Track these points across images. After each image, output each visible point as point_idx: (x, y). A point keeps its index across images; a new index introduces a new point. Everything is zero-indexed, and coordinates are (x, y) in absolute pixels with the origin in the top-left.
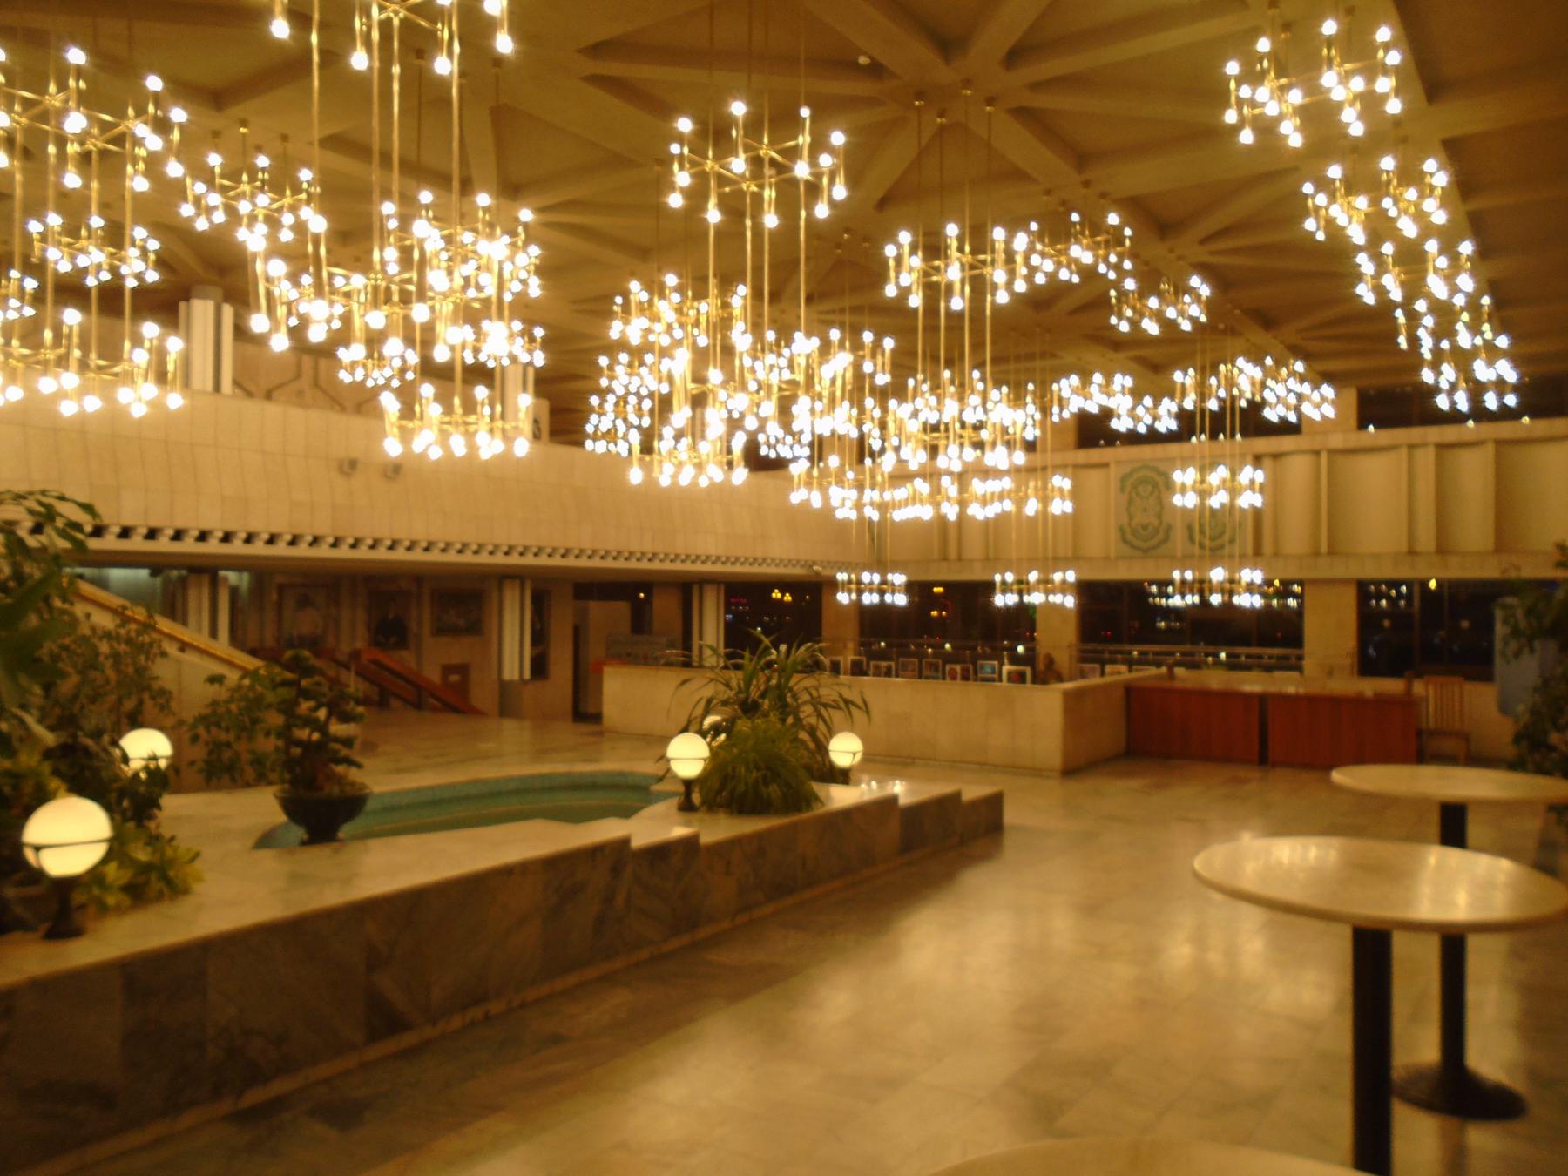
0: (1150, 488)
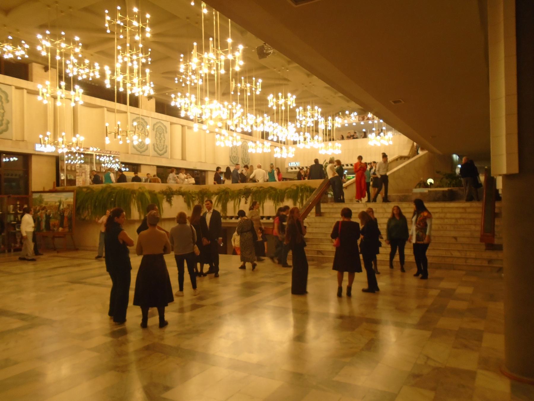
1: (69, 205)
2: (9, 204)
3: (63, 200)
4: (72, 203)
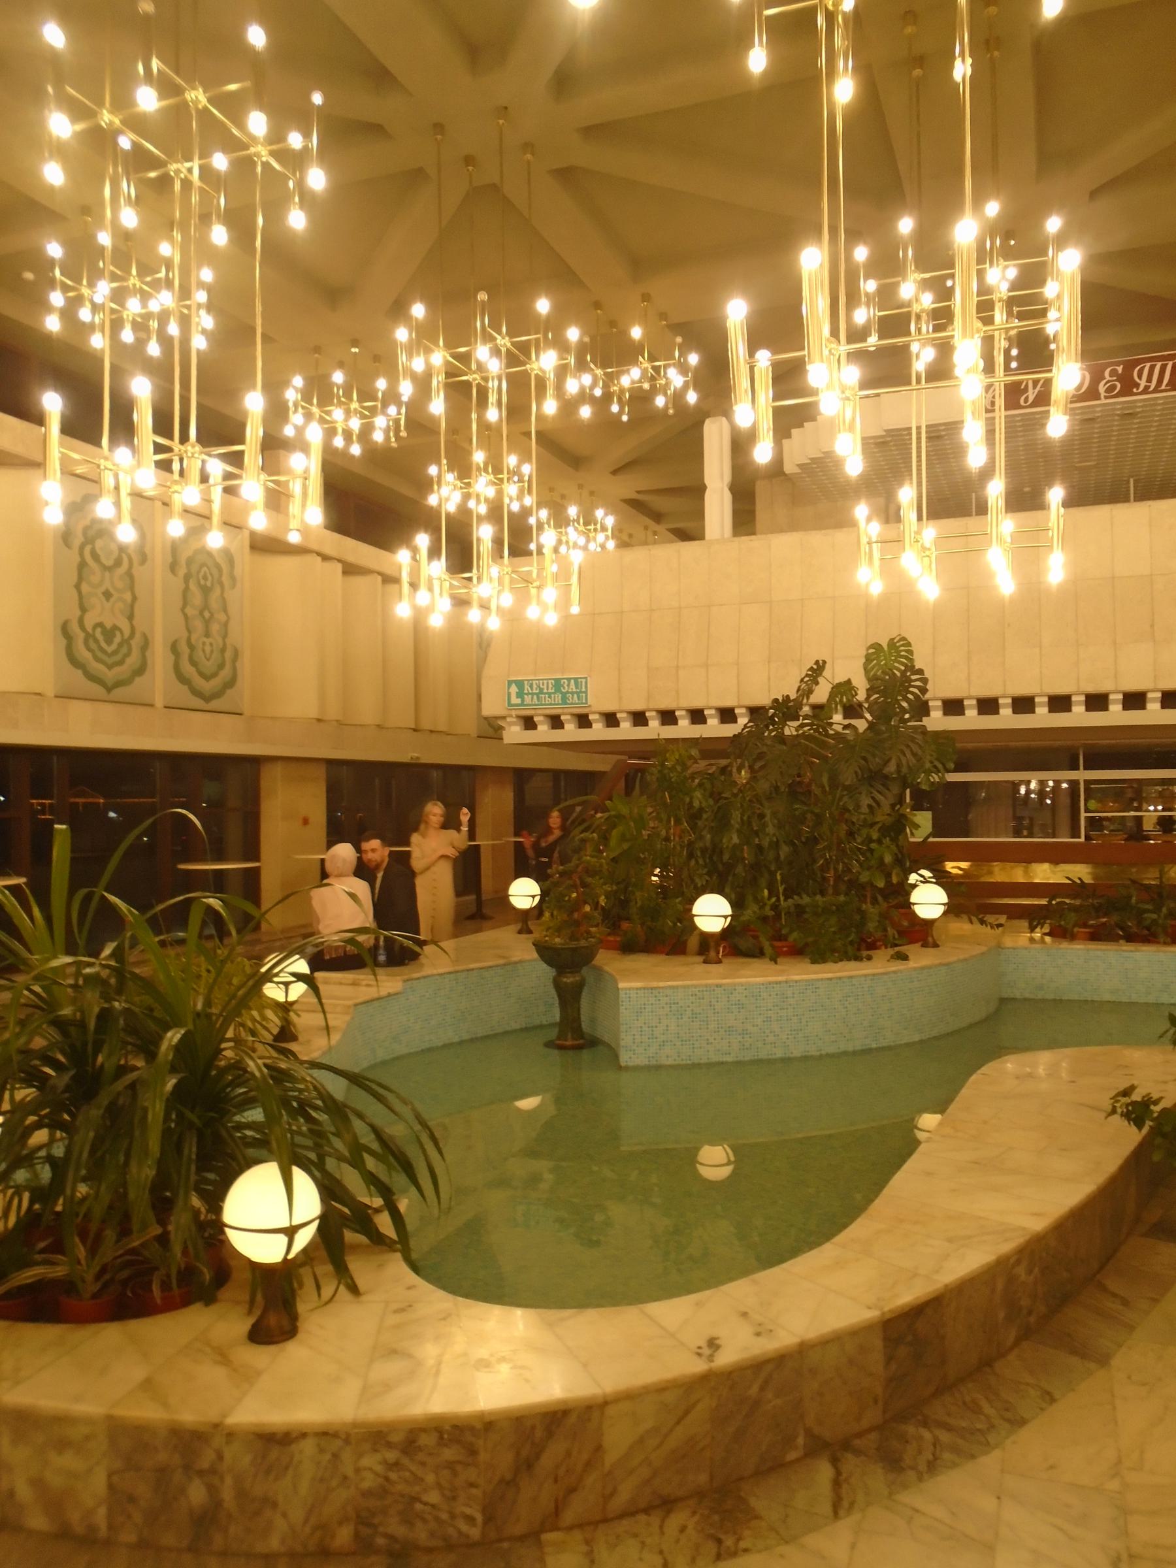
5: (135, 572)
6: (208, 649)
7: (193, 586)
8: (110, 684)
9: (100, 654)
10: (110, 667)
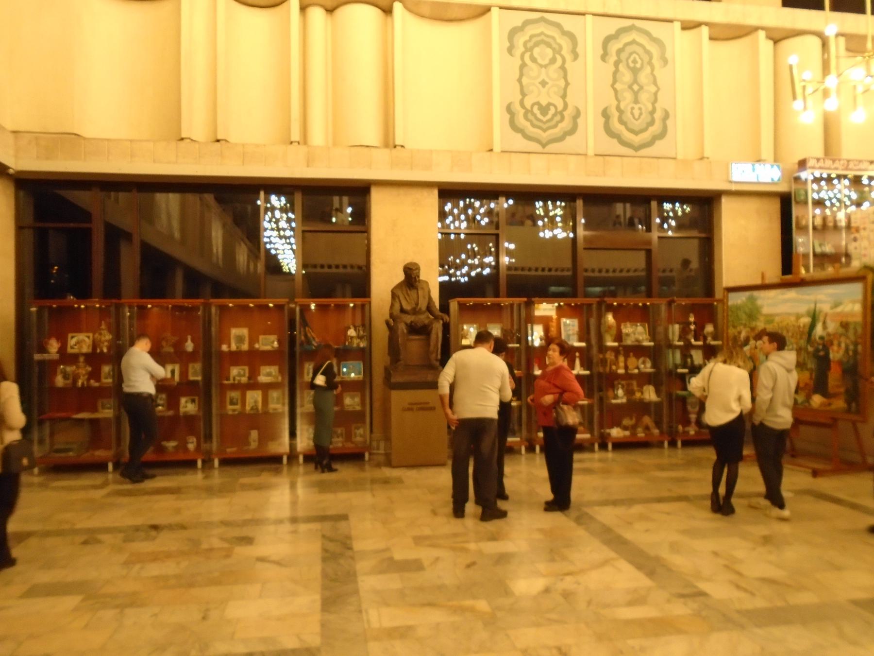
0: (549, 52)
1: (845, 326)
2: (670, 321)
3: (825, 307)
4: (859, 319)
5: (566, 66)
6: (636, 112)
7: (622, 67)
8: (544, 142)
9: (535, 122)
10: (545, 131)
